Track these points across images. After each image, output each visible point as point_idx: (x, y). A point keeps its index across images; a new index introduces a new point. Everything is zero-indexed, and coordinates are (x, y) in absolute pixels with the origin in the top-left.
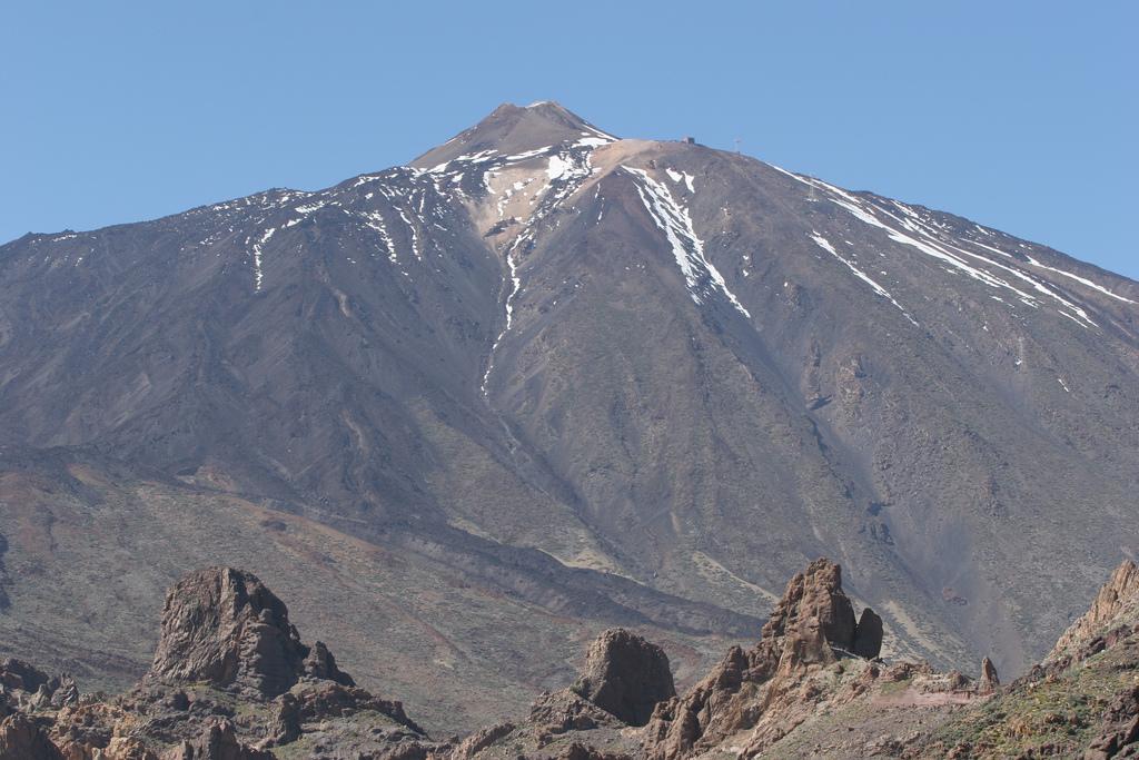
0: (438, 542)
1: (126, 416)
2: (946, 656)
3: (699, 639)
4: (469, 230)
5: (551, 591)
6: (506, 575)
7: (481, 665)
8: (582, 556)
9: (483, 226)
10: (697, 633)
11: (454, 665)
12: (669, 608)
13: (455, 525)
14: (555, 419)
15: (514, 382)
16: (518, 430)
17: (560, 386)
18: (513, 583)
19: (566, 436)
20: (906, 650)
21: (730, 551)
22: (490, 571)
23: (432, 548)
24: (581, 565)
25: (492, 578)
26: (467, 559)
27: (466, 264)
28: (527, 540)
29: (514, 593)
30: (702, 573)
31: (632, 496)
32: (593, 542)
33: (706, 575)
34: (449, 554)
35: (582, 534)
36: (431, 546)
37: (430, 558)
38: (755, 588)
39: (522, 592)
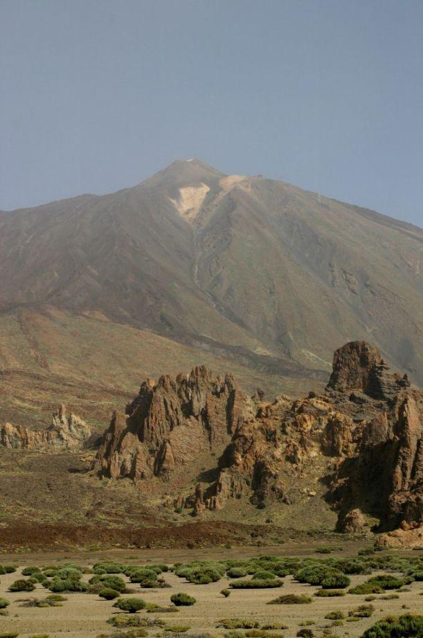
1: (51, 289)
5: (260, 364)
14: (230, 291)
16: (215, 299)
26: (221, 350)
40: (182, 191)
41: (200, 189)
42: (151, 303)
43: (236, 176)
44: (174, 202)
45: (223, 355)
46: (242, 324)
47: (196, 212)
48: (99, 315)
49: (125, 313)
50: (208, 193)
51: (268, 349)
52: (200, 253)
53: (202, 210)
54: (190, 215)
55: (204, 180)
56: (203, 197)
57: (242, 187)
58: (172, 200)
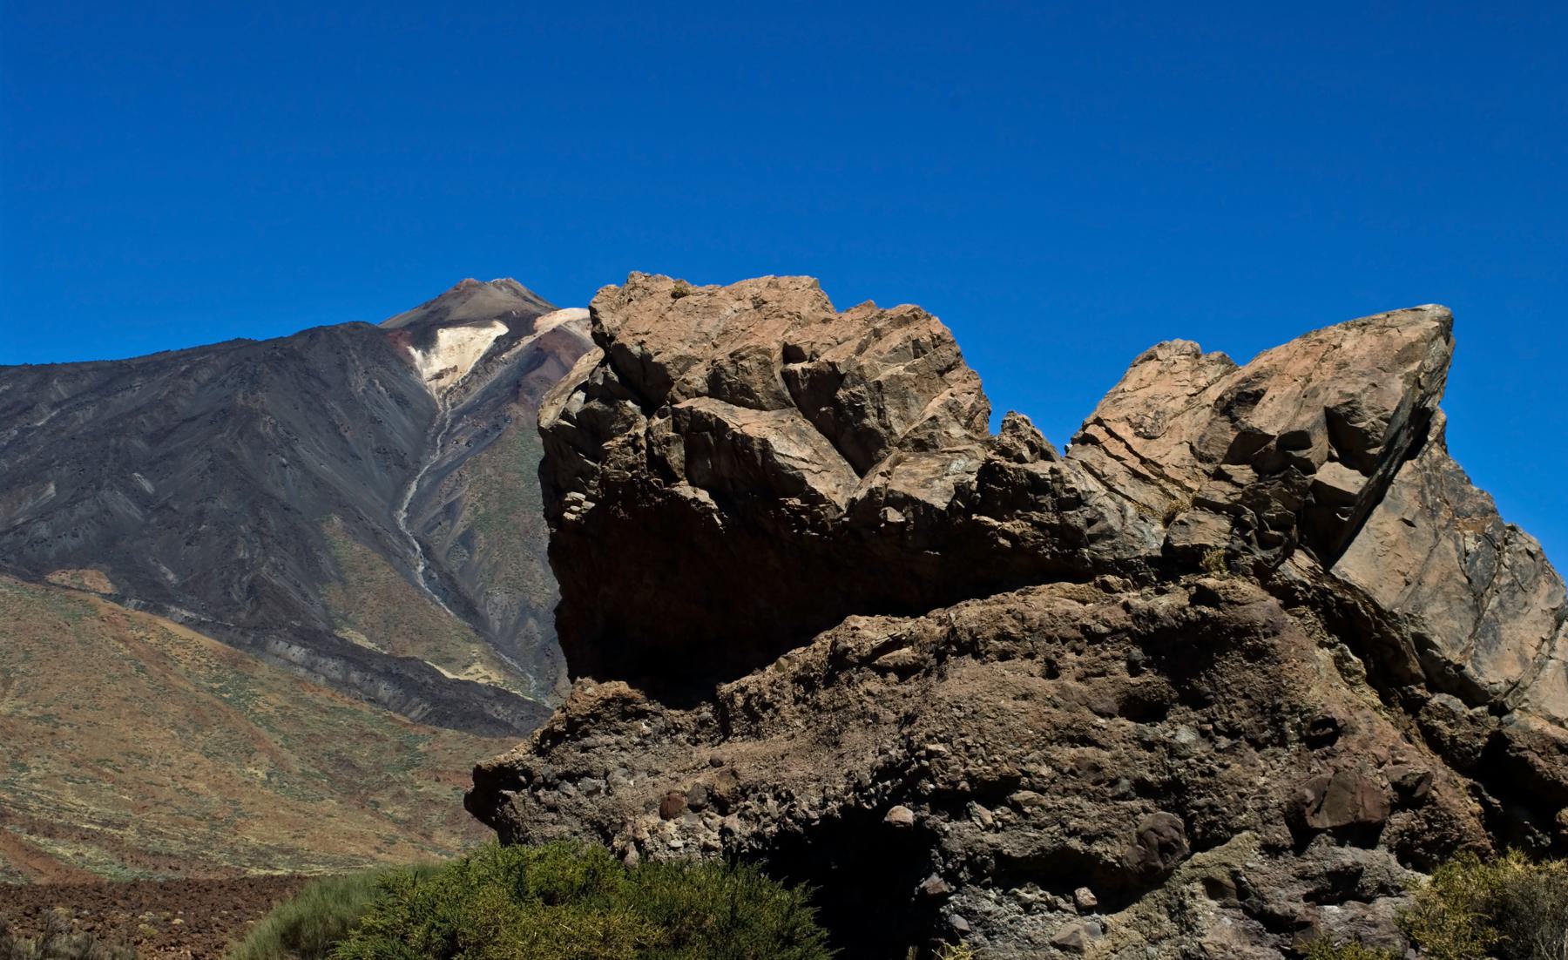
4: (414, 375)
5: (416, 700)
8: (471, 670)
9: (427, 373)
11: (269, 775)
13: (341, 635)
14: (466, 540)
15: (433, 508)
16: (427, 552)
17: (477, 509)
18: (377, 690)
19: (476, 558)
22: (355, 676)
23: (297, 652)
24: (462, 677)
26: (332, 664)
27: (401, 400)
31: (535, 615)
35: (476, 649)
36: (295, 649)
40: (445, 336)
41: (485, 331)
42: (242, 554)
43: (576, 309)
44: (417, 354)
45: (336, 675)
46: (468, 610)
47: (458, 377)
48: (98, 581)
49: (171, 577)
50: (498, 339)
51: (504, 667)
52: (435, 458)
53: (474, 372)
54: (446, 382)
55: (504, 317)
56: (485, 348)
57: (575, 329)
58: (412, 350)
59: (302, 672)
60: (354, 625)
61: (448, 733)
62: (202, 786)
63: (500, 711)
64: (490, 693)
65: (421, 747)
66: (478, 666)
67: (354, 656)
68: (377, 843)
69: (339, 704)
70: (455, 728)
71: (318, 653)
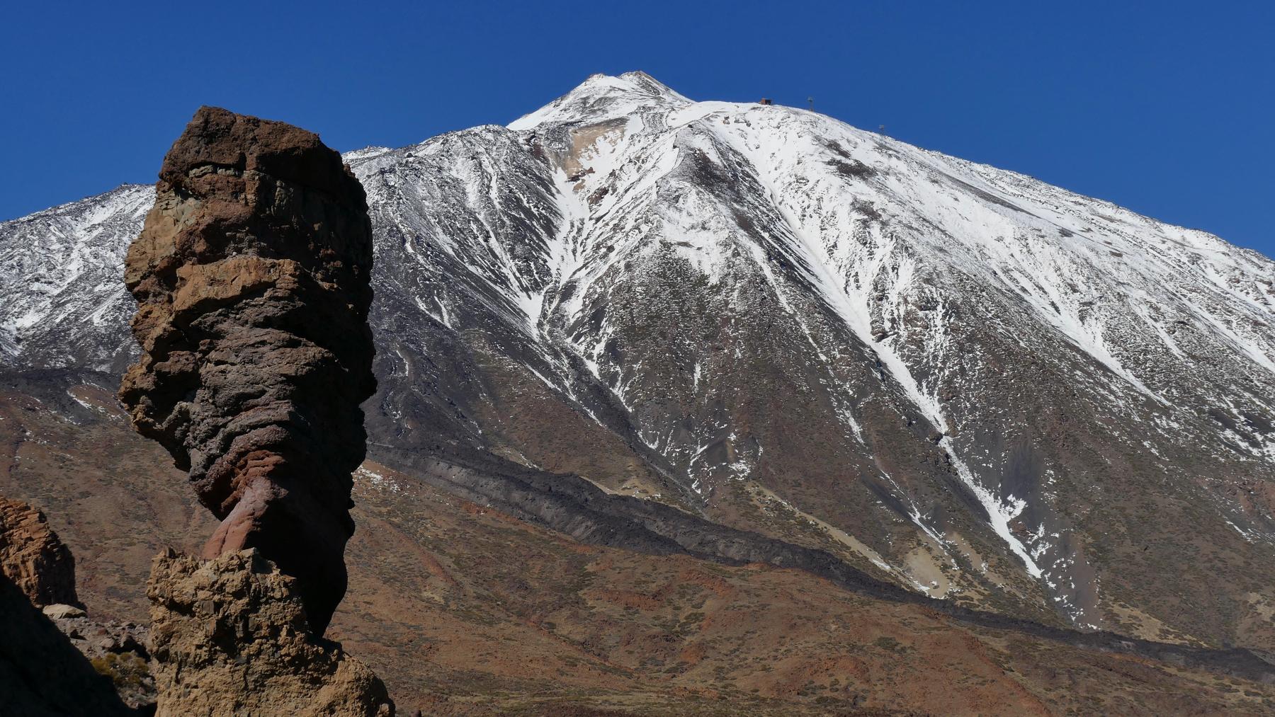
0: (464, 466)
2: (1014, 591)
3: (732, 569)
6: (533, 500)
7: (478, 597)
8: (627, 485)
10: (735, 563)
12: (710, 537)
13: (496, 453)
20: (971, 584)
21: (785, 481)
22: (517, 496)
23: (457, 473)
25: (517, 504)
26: (493, 484)
28: (572, 466)
29: (539, 519)
30: (756, 502)
32: (642, 472)
33: (758, 504)
34: (474, 478)
35: (631, 463)
36: (456, 469)
37: (452, 483)
38: (811, 520)
39: (548, 519)
59: (463, 493)
60: (509, 443)
61: (614, 553)
62: (385, 612)
63: (658, 527)
64: (649, 508)
65: (590, 567)
66: (633, 481)
67: (514, 476)
68: (560, 664)
69: (504, 525)
70: (620, 546)
71: (479, 472)
